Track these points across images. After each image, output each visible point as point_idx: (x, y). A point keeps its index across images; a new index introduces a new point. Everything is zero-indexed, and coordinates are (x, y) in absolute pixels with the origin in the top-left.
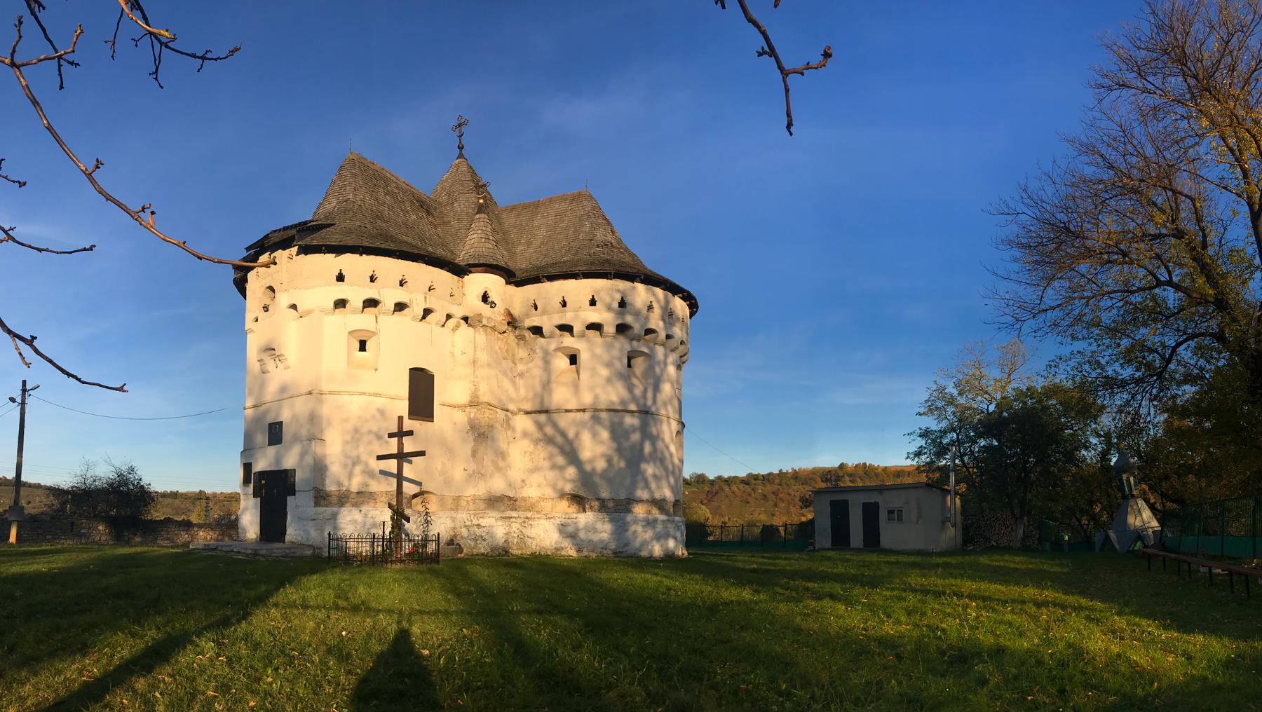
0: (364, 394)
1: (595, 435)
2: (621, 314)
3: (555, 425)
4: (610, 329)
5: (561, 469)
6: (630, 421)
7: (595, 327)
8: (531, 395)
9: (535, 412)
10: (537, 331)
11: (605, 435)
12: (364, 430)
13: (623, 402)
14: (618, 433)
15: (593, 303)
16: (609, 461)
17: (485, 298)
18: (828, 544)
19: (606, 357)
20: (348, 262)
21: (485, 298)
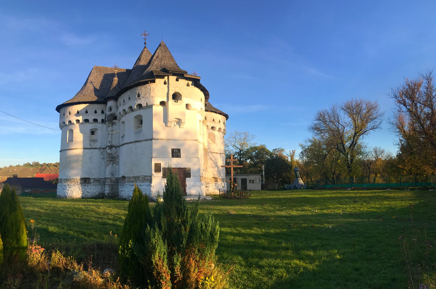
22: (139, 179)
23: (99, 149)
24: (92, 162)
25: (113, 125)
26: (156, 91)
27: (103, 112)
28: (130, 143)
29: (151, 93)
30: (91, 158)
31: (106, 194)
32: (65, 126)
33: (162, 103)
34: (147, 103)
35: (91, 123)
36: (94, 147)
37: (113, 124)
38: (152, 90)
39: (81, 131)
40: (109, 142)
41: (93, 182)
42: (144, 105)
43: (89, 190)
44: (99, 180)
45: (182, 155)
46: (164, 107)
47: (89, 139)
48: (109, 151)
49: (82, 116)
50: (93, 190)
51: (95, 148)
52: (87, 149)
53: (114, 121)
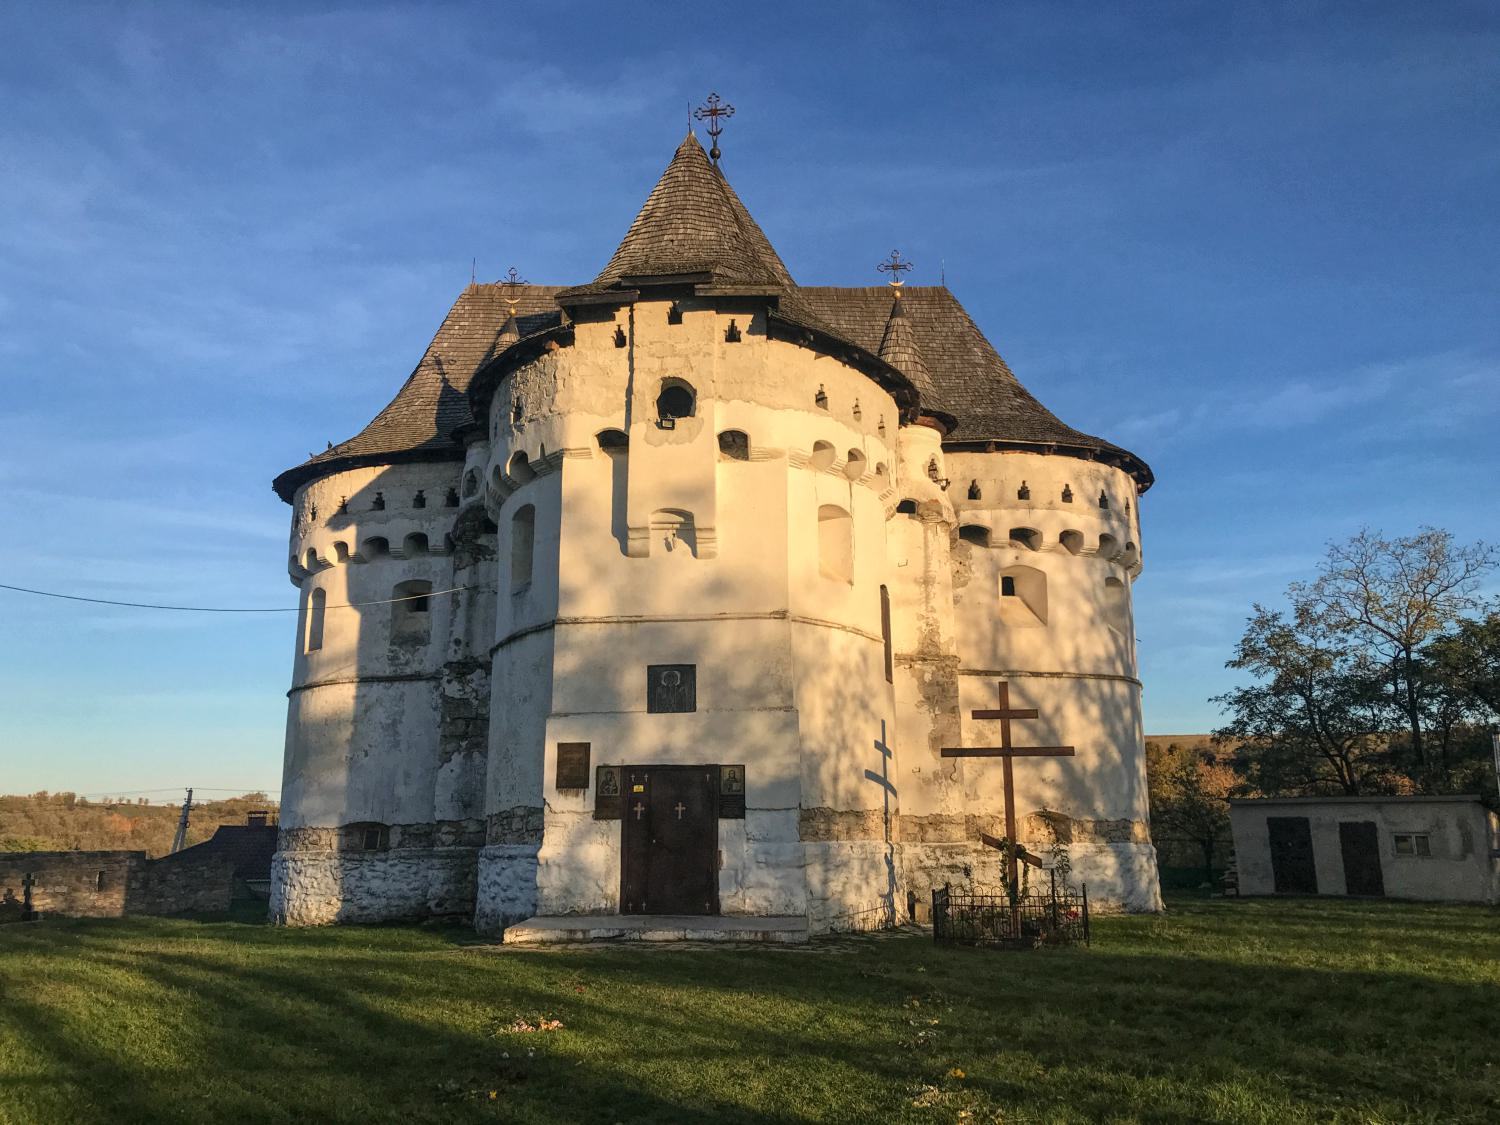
0: (844, 628)
1: (1083, 710)
2: (1106, 517)
4: (1091, 541)
6: (1121, 689)
7: (1069, 539)
8: (973, 636)
9: (987, 673)
10: (975, 534)
11: (1094, 711)
12: (848, 691)
13: (1111, 661)
14: (1110, 711)
15: (1067, 496)
16: (1103, 754)
17: (932, 469)
18: (1269, 888)
19: (1087, 583)
21: (932, 469)
22: (510, 824)
23: (435, 677)
24: (396, 745)
25: (477, 561)
26: (576, 383)
27: (453, 500)
28: (501, 645)
29: (558, 397)
30: (393, 726)
31: (432, 904)
32: (304, 573)
33: (614, 441)
34: (542, 445)
35: (399, 556)
36: (408, 671)
37: (481, 553)
38: (560, 382)
39: (355, 600)
40: (457, 642)
41: (400, 845)
42: (534, 456)
43: (376, 884)
44: (428, 835)
45: (702, 700)
46: (621, 457)
47: (387, 633)
48: (453, 690)
49: (357, 525)
50: (395, 880)
51: (416, 677)
52: (379, 680)
53: (482, 540)
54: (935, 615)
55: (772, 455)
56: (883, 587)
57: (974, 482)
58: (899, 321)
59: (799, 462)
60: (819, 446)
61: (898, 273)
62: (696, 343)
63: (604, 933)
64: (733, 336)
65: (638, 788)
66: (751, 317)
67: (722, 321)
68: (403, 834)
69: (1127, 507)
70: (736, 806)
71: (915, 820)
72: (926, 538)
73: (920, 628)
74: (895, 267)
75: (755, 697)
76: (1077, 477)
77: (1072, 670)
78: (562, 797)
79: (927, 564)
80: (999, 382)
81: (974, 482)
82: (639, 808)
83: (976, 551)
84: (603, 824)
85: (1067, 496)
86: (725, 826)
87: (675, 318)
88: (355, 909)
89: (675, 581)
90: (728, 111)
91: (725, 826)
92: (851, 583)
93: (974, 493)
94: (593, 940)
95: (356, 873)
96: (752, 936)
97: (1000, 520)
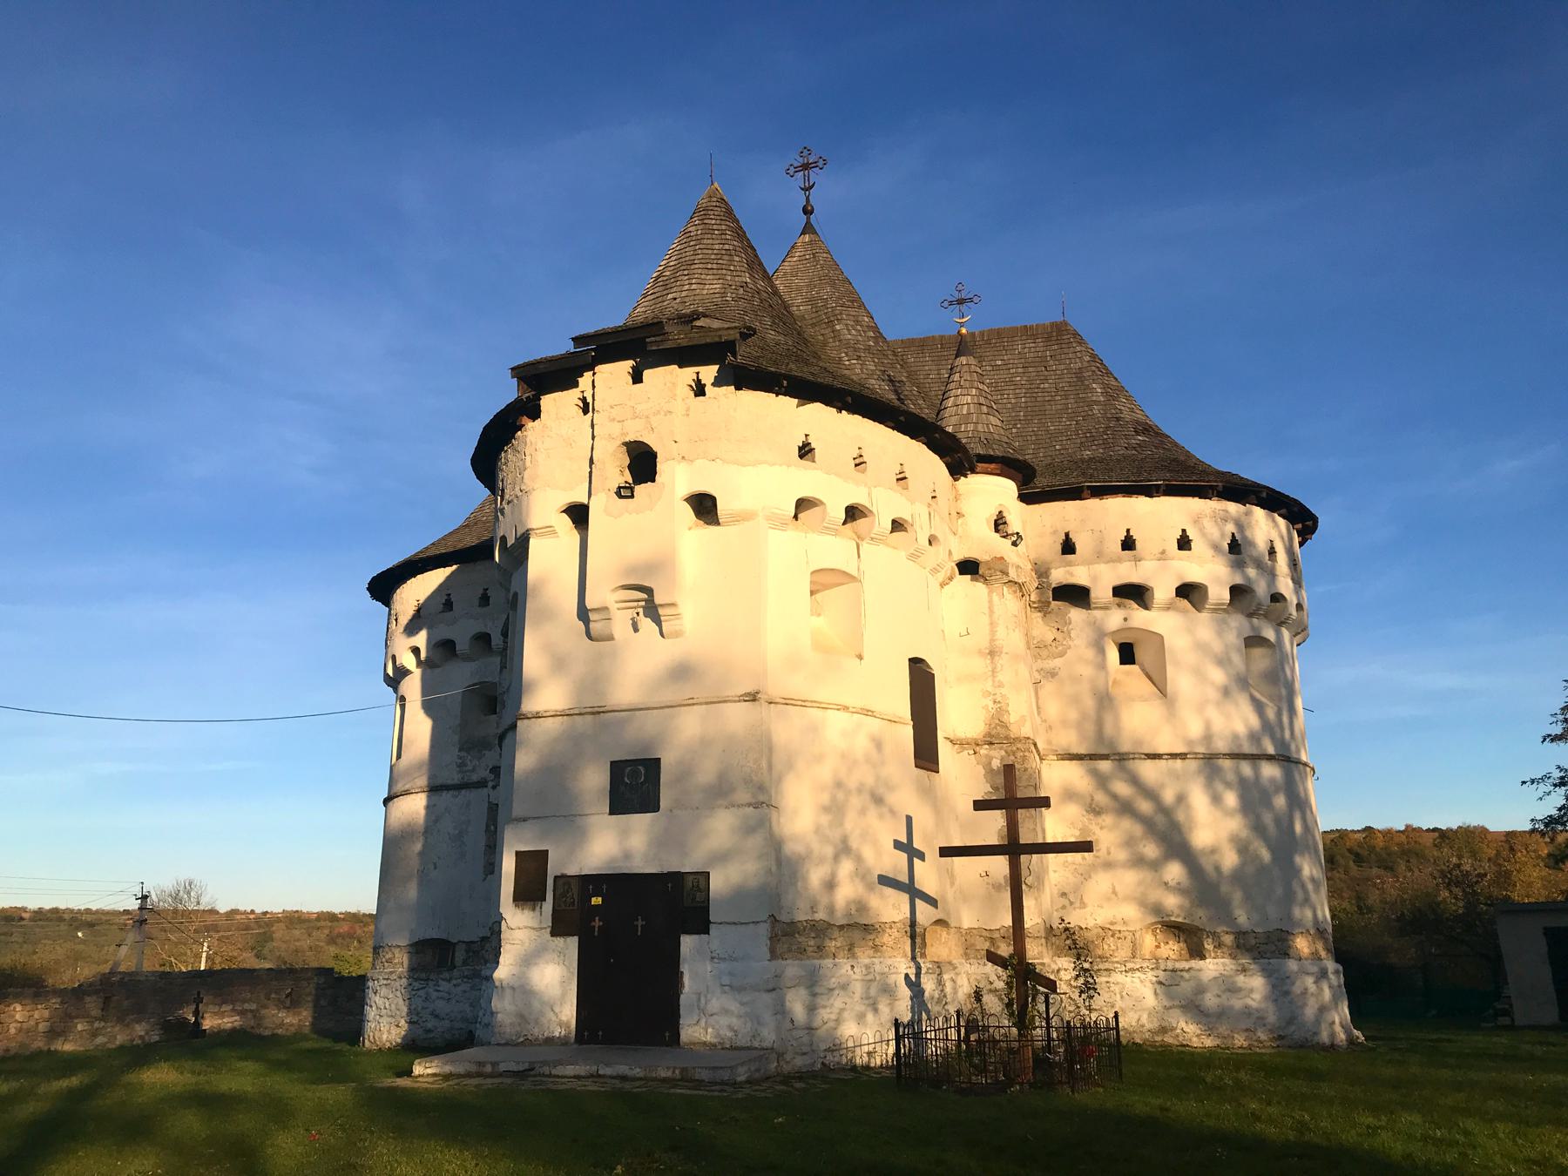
0: (846, 708)
1: (1216, 800)
2: (1239, 565)
3: (1135, 781)
4: (1219, 593)
5: (1155, 866)
6: (1270, 771)
7: (1189, 592)
8: (1073, 715)
9: (1092, 757)
10: (1076, 595)
11: (1231, 799)
12: (852, 783)
13: (1254, 737)
14: (1253, 800)
15: (1184, 543)
16: (1243, 848)
17: (999, 524)
19: (1217, 646)
20: (819, 419)
21: (999, 524)
33: (579, 514)
36: (475, 778)
39: (428, 707)
41: (465, 963)
45: (664, 802)
47: (456, 738)
54: (1003, 691)
55: (742, 517)
56: (916, 663)
57: (1067, 535)
58: (963, 360)
59: (777, 523)
60: (802, 504)
61: (964, 307)
62: (658, 404)
63: (513, 1067)
64: (699, 390)
65: (597, 901)
66: (716, 367)
67: (688, 374)
68: (467, 951)
69: (1272, 552)
70: (700, 923)
71: (985, 934)
72: (990, 601)
73: (986, 707)
74: (961, 302)
75: (720, 792)
76: (1197, 521)
77: (1201, 749)
78: (519, 911)
79: (993, 632)
80: (1118, 419)
81: (1067, 535)
82: (597, 923)
83: (1076, 614)
84: (560, 941)
85: (1184, 543)
86: (687, 943)
87: (637, 378)
88: (420, 1032)
89: (639, 661)
90: (821, 163)
91: (687, 943)
92: (860, 657)
93: (1068, 547)
94: (500, 1075)
95: (421, 993)
96: (669, 1074)
97: (1101, 578)
